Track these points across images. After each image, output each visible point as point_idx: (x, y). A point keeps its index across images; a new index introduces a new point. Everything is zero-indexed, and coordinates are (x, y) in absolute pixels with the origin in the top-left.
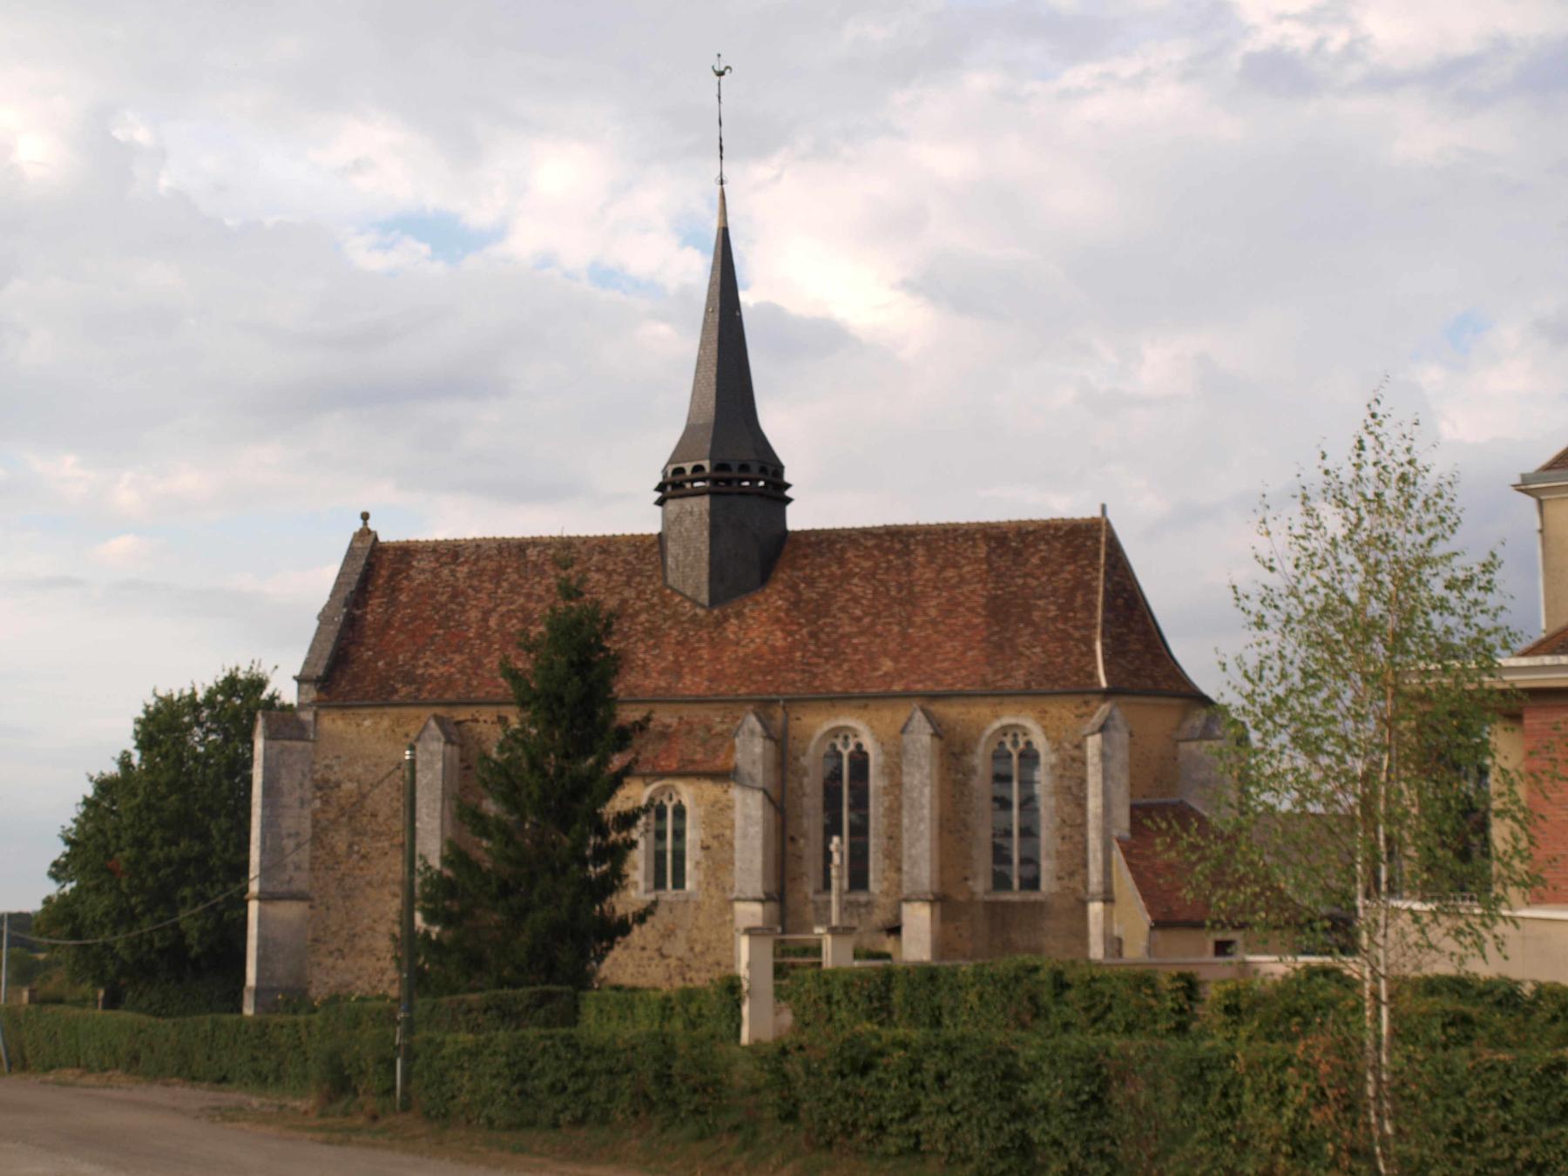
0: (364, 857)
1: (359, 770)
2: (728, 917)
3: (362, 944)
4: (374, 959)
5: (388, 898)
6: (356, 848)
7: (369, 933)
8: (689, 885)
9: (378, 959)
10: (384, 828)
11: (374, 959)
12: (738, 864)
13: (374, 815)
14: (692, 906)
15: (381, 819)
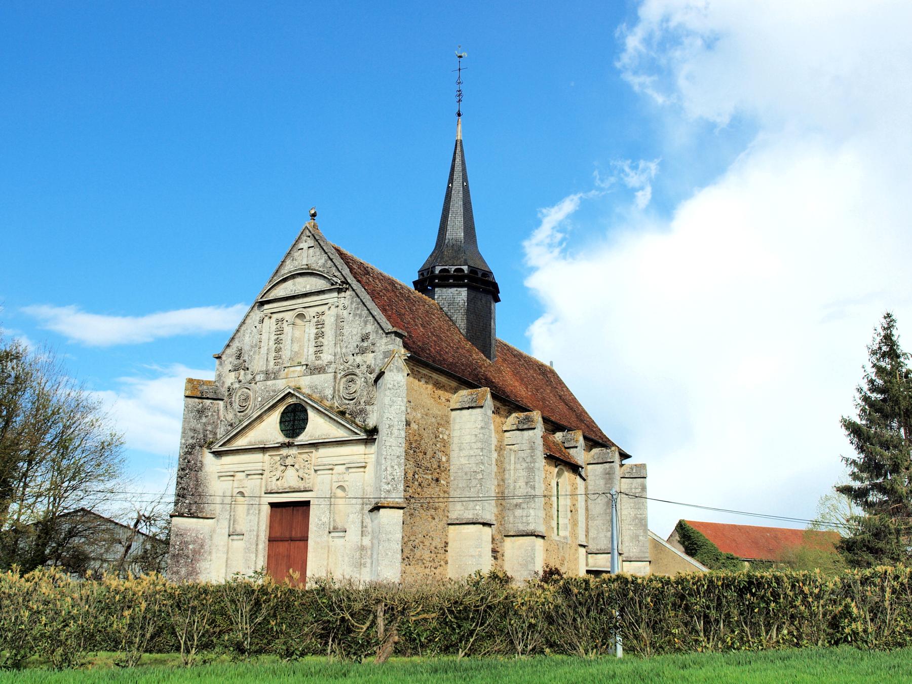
0: (420, 485)
1: (419, 416)
2: (577, 555)
3: (418, 553)
4: (423, 566)
5: (430, 519)
6: (416, 476)
7: (421, 545)
8: (561, 533)
9: (425, 567)
10: (429, 465)
11: (423, 566)
12: (579, 523)
13: (425, 454)
14: (568, 546)
15: (428, 456)
